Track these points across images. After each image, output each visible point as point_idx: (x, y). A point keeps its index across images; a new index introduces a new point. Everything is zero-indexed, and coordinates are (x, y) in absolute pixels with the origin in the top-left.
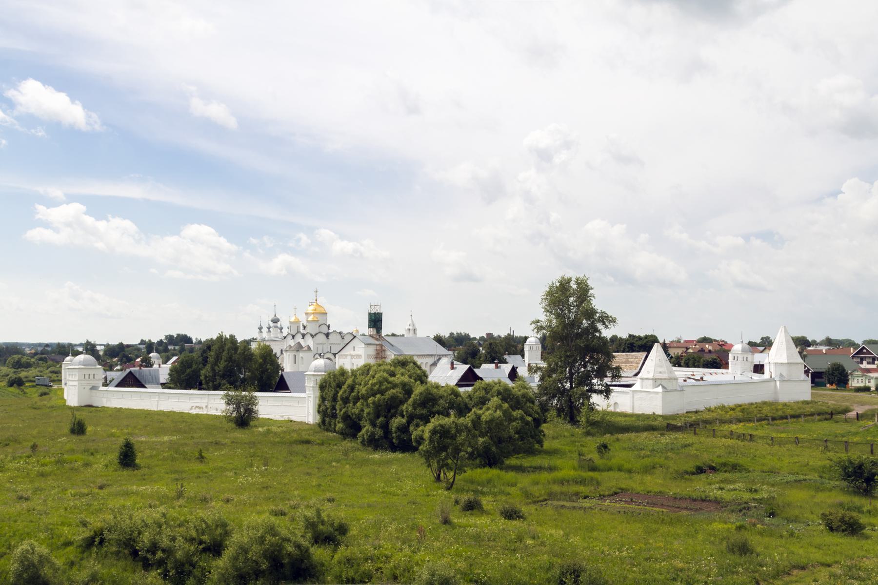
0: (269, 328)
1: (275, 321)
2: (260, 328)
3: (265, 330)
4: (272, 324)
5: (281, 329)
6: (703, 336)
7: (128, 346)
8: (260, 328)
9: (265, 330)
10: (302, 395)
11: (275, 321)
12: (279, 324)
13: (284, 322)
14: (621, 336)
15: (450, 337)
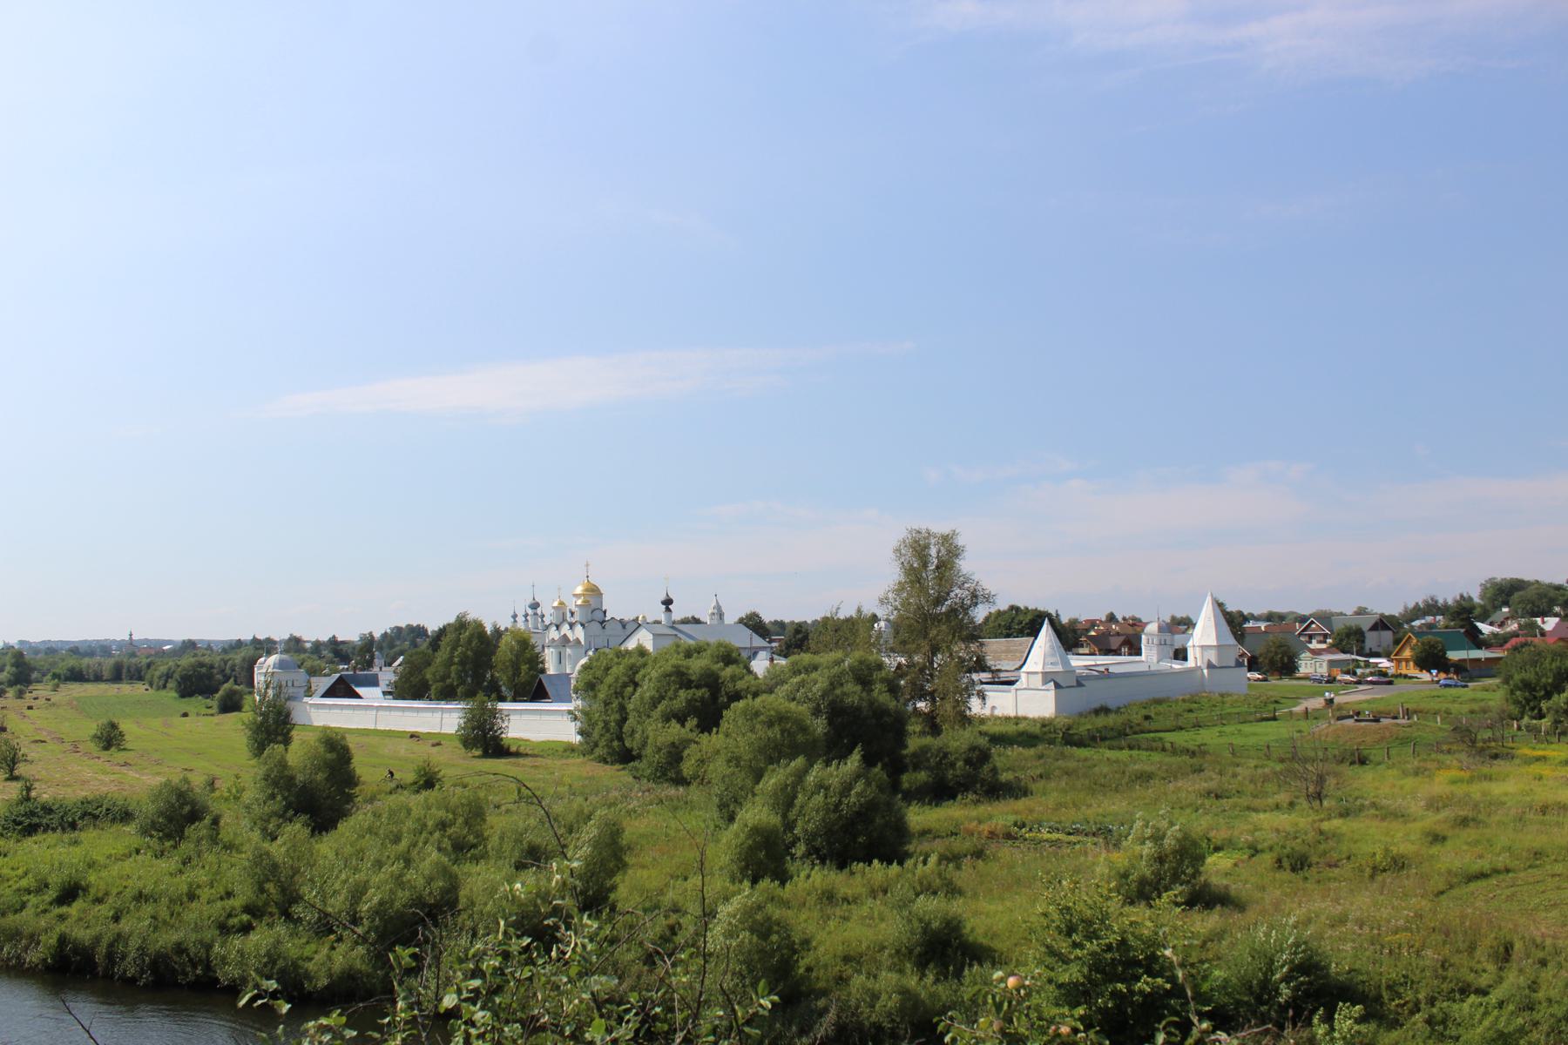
0: (526, 616)
1: (535, 606)
2: (515, 616)
3: (520, 619)
4: (530, 611)
5: (543, 616)
6: (1184, 616)
7: (1093, 624)
8: (515, 616)
9: (520, 619)
10: (1137, 658)
11: (535, 606)
12: (539, 611)
13: (547, 610)
14: (1074, 615)
15: (1414, 608)
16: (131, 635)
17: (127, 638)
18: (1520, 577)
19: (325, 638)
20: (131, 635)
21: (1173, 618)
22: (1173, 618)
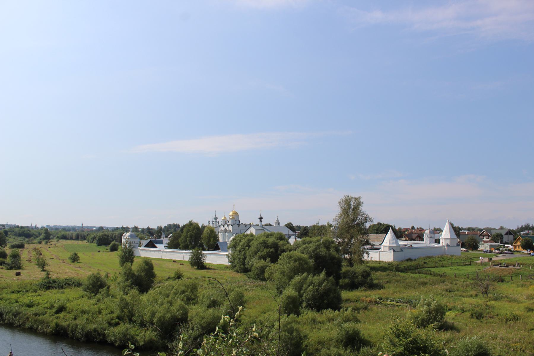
0: (213, 222)
1: (216, 218)
2: (209, 222)
3: (211, 223)
4: (214, 220)
5: (219, 222)
6: (439, 228)
7: (406, 230)
8: (209, 222)
9: (211, 223)
11: (216, 218)
12: (217, 220)
13: (220, 220)
15: (521, 227)
16: (82, 224)
17: (81, 225)
18: (488, 227)
19: (146, 227)
20: (82, 224)
21: (435, 228)
22: (435, 228)
